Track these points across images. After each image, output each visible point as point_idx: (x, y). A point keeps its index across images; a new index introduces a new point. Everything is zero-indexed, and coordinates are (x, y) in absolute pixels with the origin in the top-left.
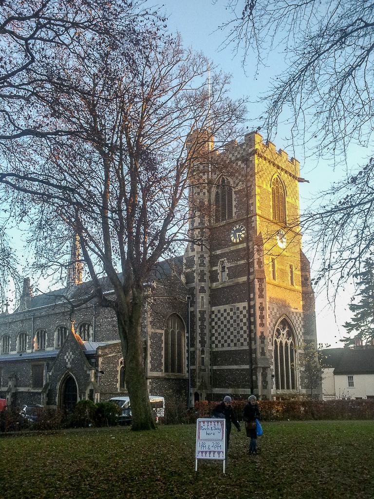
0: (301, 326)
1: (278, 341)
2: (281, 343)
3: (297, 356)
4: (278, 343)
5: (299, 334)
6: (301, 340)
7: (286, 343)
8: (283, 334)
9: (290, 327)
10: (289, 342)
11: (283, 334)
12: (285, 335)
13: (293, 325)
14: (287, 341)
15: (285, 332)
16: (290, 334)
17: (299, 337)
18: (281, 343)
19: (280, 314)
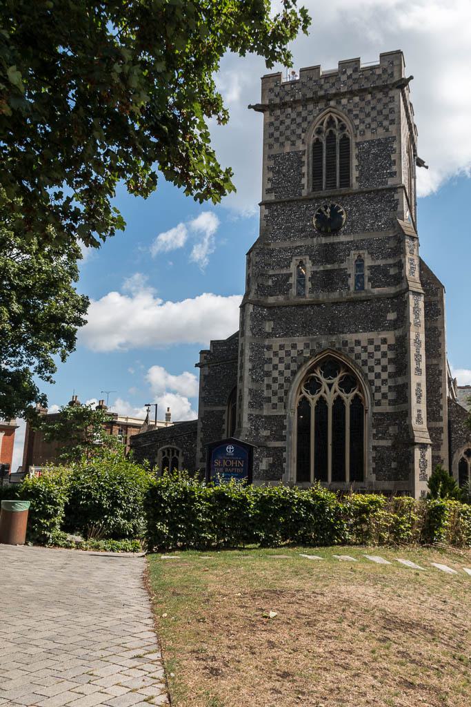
0: (384, 362)
1: (313, 400)
2: (322, 401)
3: (368, 419)
4: (313, 404)
5: (378, 376)
6: (385, 389)
7: (339, 401)
8: (330, 386)
9: (348, 369)
10: (348, 398)
11: (330, 386)
12: (336, 386)
13: (356, 365)
14: (344, 395)
15: (336, 381)
16: (349, 382)
17: (378, 383)
18: (322, 401)
19: (312, 351)
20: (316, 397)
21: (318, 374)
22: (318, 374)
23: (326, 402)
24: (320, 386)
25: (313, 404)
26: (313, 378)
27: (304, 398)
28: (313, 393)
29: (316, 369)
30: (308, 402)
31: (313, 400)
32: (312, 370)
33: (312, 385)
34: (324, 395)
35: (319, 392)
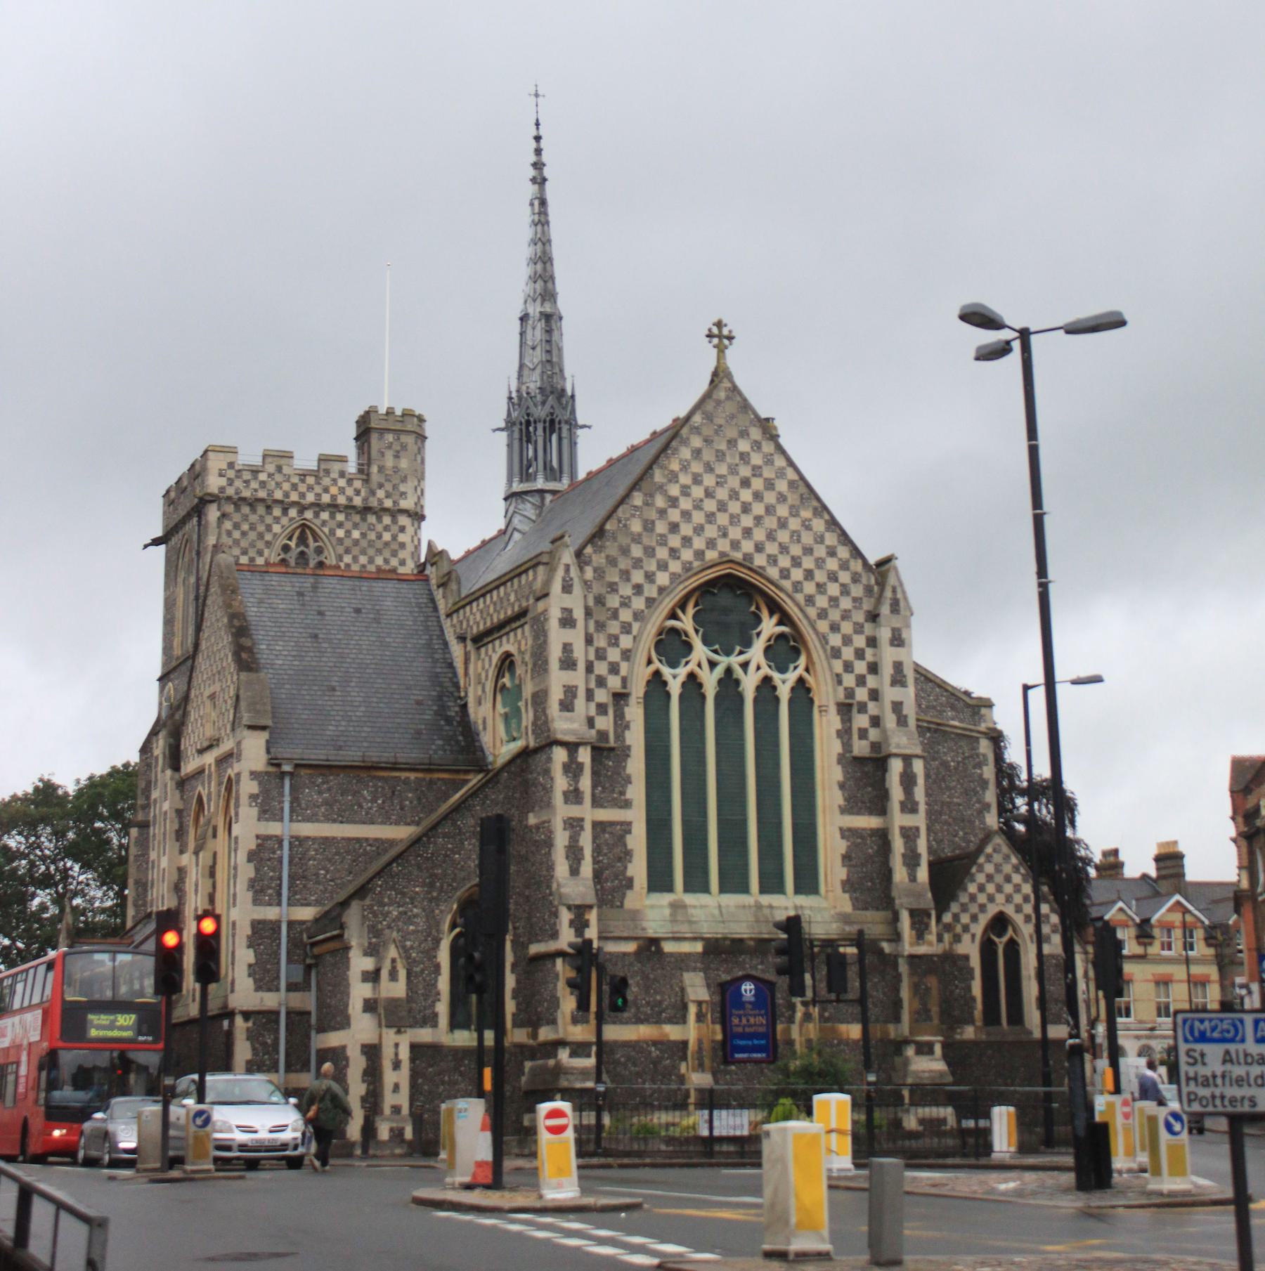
1: (675, 680)
4: (675, 688)
20: (682, 672)
21: (686, 623)
22: (686, 623)
23: (700, 685)
24: (689, 647)
25: (675, 688)
26: (674, 631)
27: (657, 674)
28: (673, 664)
29: (684, 611)
30: (665, 683)
31: (675, 680)
32: (673, 616)
33: (672, 645)
34: (697, 670)
35: (687, 663)
